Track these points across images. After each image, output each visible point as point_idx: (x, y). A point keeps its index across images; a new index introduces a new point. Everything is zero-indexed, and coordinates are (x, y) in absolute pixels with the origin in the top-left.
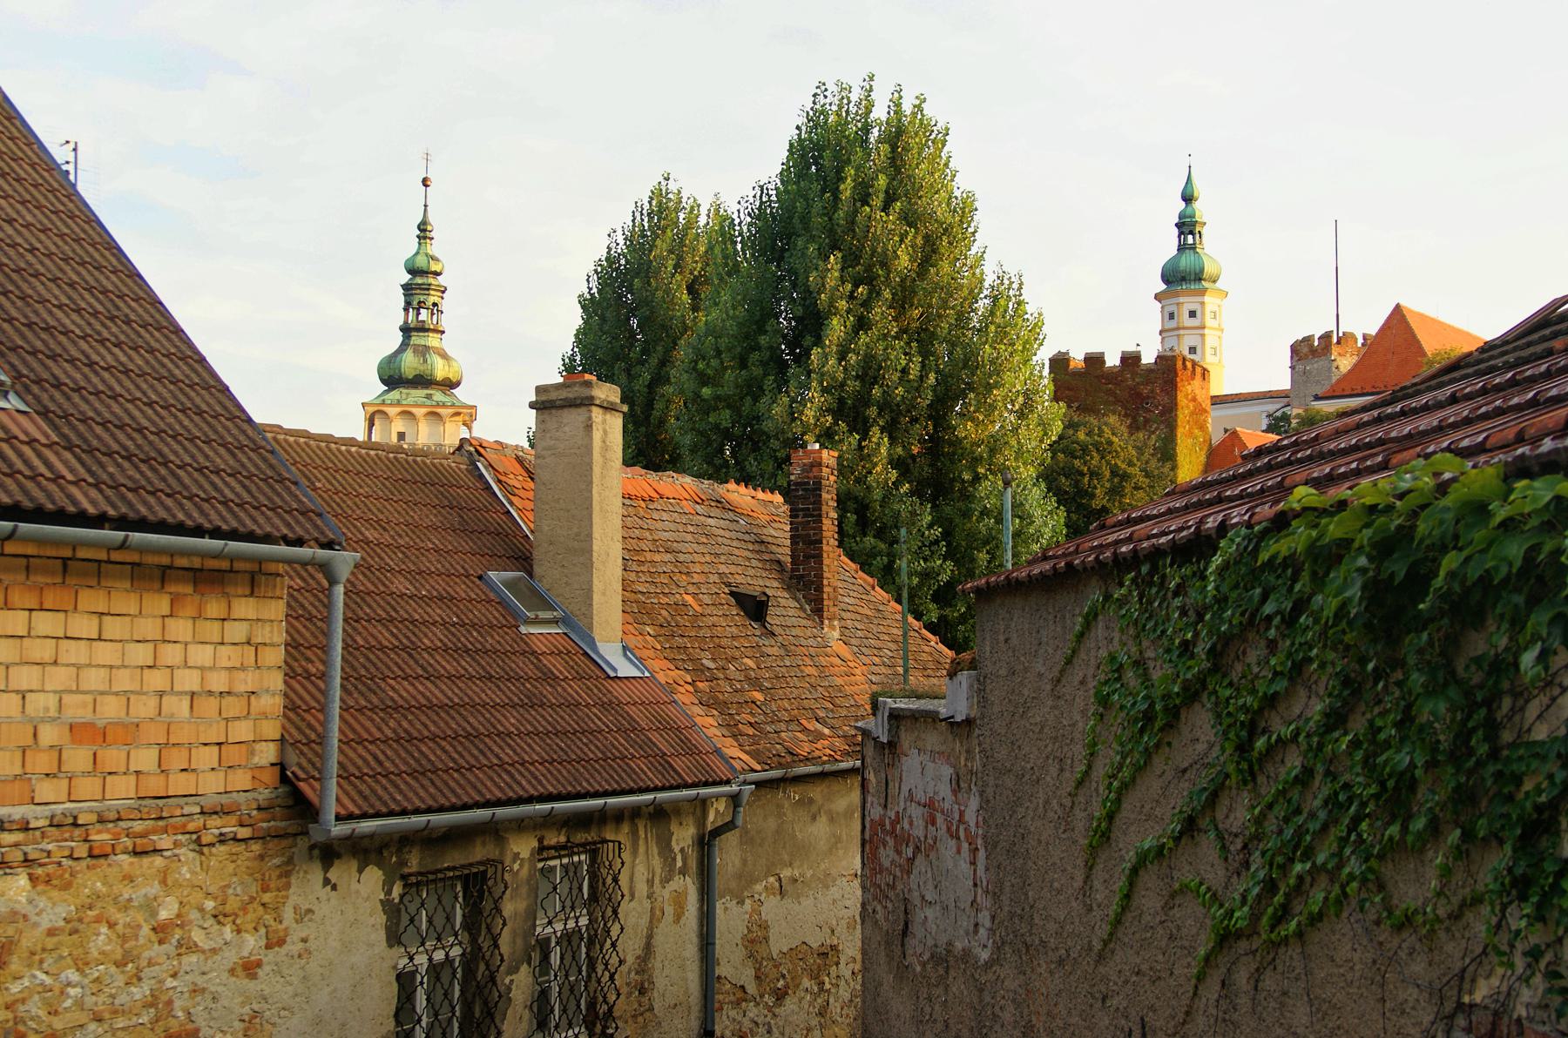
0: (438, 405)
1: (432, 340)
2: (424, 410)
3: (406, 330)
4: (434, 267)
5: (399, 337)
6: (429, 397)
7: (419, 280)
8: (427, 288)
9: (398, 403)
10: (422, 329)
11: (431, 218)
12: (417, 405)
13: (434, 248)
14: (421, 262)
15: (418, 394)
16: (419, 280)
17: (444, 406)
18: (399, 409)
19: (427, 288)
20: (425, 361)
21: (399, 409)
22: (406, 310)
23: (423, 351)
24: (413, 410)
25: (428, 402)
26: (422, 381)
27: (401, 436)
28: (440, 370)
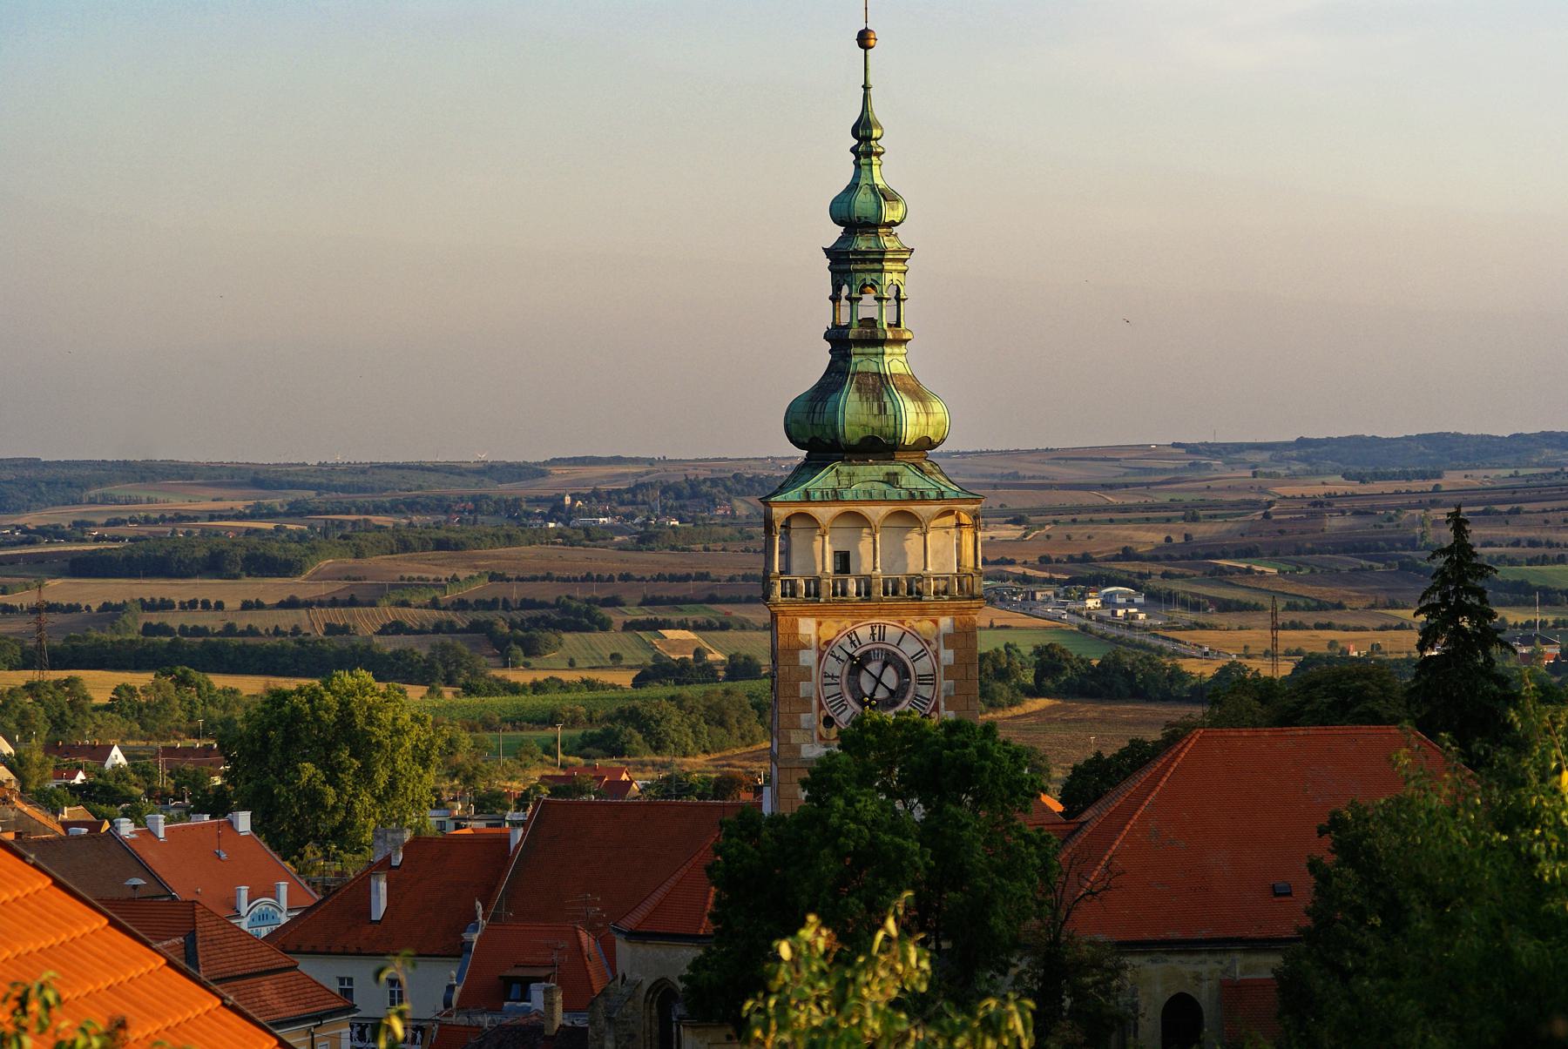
0: (912, 498)
1: (894, 362)
2: (884, 510)
3: (838, 339)
4: (890, 214)
5: (822, 356)
6: (891, 480)
7: (862, 244)
8: (879, 256)
9: (836, 497)
10: (872, 337)
11: (878, 111)
12: (872, 501)
13: (882, 174)
14: (863, 203)
15: (869, 475)
16: (862, 244)
17: (923, 499)
18: (837, 509)
19: (878, 257)
20: (882, 409)
21: (837, 509)
22: (835, 298)
23: (878, 386)
24: (866, 510)
25: (893, 493)
26: (881, 446)
27: (844, 561)
28: (913, 422)
